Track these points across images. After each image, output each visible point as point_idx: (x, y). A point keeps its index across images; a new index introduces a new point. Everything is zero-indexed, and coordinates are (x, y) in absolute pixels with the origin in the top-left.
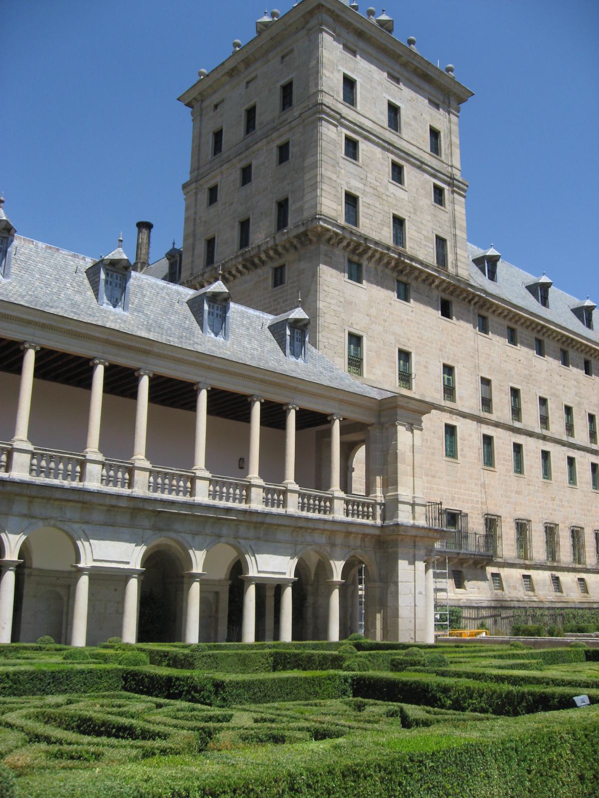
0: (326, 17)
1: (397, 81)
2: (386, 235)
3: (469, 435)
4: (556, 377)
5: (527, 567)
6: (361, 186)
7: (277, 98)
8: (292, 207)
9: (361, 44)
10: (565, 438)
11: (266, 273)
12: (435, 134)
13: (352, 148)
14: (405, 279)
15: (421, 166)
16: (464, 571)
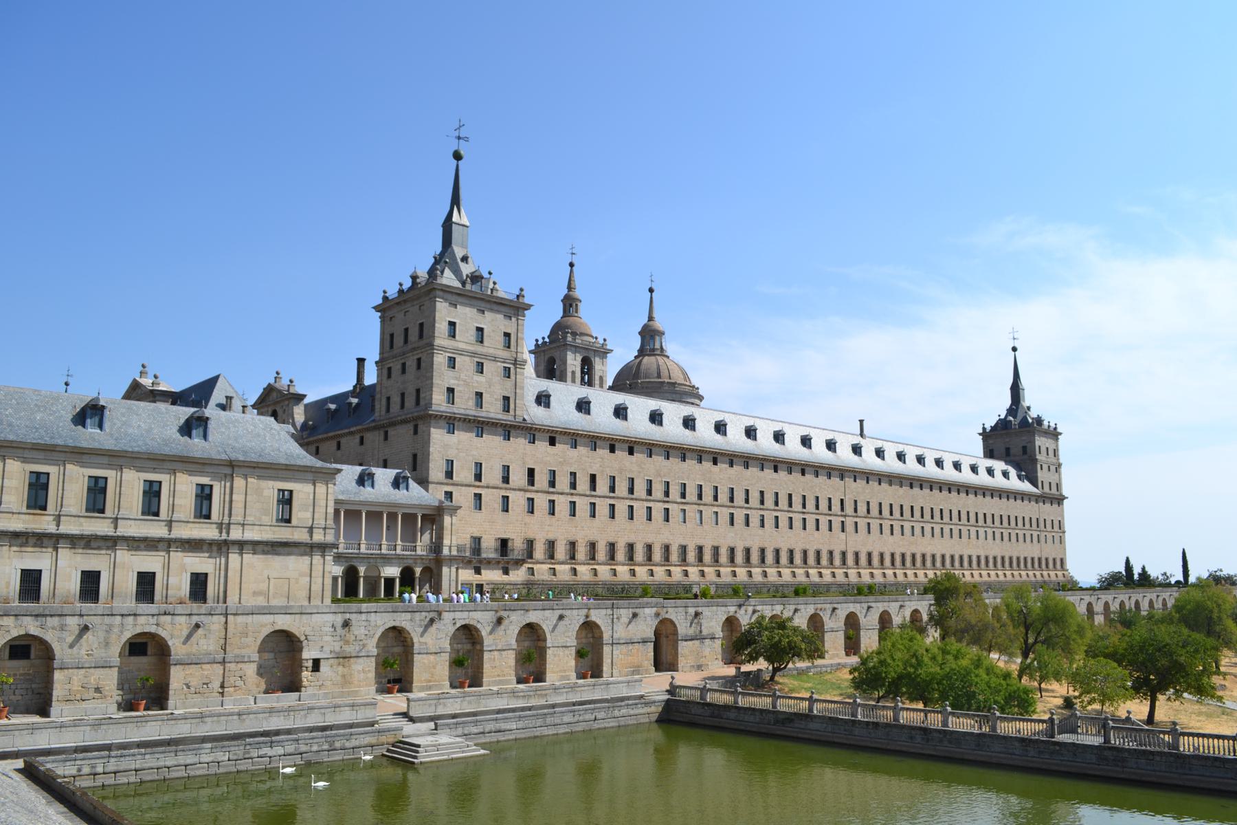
0: (438, 293)
1: (483, 312)
7: (417, 329)
8: (422, 395)
9: (460, 299)
10: (588, 493)
11: (410, 427)
12: (507, 335)
13: (452, 363)
14: (480, 426)
15: (495, 359)
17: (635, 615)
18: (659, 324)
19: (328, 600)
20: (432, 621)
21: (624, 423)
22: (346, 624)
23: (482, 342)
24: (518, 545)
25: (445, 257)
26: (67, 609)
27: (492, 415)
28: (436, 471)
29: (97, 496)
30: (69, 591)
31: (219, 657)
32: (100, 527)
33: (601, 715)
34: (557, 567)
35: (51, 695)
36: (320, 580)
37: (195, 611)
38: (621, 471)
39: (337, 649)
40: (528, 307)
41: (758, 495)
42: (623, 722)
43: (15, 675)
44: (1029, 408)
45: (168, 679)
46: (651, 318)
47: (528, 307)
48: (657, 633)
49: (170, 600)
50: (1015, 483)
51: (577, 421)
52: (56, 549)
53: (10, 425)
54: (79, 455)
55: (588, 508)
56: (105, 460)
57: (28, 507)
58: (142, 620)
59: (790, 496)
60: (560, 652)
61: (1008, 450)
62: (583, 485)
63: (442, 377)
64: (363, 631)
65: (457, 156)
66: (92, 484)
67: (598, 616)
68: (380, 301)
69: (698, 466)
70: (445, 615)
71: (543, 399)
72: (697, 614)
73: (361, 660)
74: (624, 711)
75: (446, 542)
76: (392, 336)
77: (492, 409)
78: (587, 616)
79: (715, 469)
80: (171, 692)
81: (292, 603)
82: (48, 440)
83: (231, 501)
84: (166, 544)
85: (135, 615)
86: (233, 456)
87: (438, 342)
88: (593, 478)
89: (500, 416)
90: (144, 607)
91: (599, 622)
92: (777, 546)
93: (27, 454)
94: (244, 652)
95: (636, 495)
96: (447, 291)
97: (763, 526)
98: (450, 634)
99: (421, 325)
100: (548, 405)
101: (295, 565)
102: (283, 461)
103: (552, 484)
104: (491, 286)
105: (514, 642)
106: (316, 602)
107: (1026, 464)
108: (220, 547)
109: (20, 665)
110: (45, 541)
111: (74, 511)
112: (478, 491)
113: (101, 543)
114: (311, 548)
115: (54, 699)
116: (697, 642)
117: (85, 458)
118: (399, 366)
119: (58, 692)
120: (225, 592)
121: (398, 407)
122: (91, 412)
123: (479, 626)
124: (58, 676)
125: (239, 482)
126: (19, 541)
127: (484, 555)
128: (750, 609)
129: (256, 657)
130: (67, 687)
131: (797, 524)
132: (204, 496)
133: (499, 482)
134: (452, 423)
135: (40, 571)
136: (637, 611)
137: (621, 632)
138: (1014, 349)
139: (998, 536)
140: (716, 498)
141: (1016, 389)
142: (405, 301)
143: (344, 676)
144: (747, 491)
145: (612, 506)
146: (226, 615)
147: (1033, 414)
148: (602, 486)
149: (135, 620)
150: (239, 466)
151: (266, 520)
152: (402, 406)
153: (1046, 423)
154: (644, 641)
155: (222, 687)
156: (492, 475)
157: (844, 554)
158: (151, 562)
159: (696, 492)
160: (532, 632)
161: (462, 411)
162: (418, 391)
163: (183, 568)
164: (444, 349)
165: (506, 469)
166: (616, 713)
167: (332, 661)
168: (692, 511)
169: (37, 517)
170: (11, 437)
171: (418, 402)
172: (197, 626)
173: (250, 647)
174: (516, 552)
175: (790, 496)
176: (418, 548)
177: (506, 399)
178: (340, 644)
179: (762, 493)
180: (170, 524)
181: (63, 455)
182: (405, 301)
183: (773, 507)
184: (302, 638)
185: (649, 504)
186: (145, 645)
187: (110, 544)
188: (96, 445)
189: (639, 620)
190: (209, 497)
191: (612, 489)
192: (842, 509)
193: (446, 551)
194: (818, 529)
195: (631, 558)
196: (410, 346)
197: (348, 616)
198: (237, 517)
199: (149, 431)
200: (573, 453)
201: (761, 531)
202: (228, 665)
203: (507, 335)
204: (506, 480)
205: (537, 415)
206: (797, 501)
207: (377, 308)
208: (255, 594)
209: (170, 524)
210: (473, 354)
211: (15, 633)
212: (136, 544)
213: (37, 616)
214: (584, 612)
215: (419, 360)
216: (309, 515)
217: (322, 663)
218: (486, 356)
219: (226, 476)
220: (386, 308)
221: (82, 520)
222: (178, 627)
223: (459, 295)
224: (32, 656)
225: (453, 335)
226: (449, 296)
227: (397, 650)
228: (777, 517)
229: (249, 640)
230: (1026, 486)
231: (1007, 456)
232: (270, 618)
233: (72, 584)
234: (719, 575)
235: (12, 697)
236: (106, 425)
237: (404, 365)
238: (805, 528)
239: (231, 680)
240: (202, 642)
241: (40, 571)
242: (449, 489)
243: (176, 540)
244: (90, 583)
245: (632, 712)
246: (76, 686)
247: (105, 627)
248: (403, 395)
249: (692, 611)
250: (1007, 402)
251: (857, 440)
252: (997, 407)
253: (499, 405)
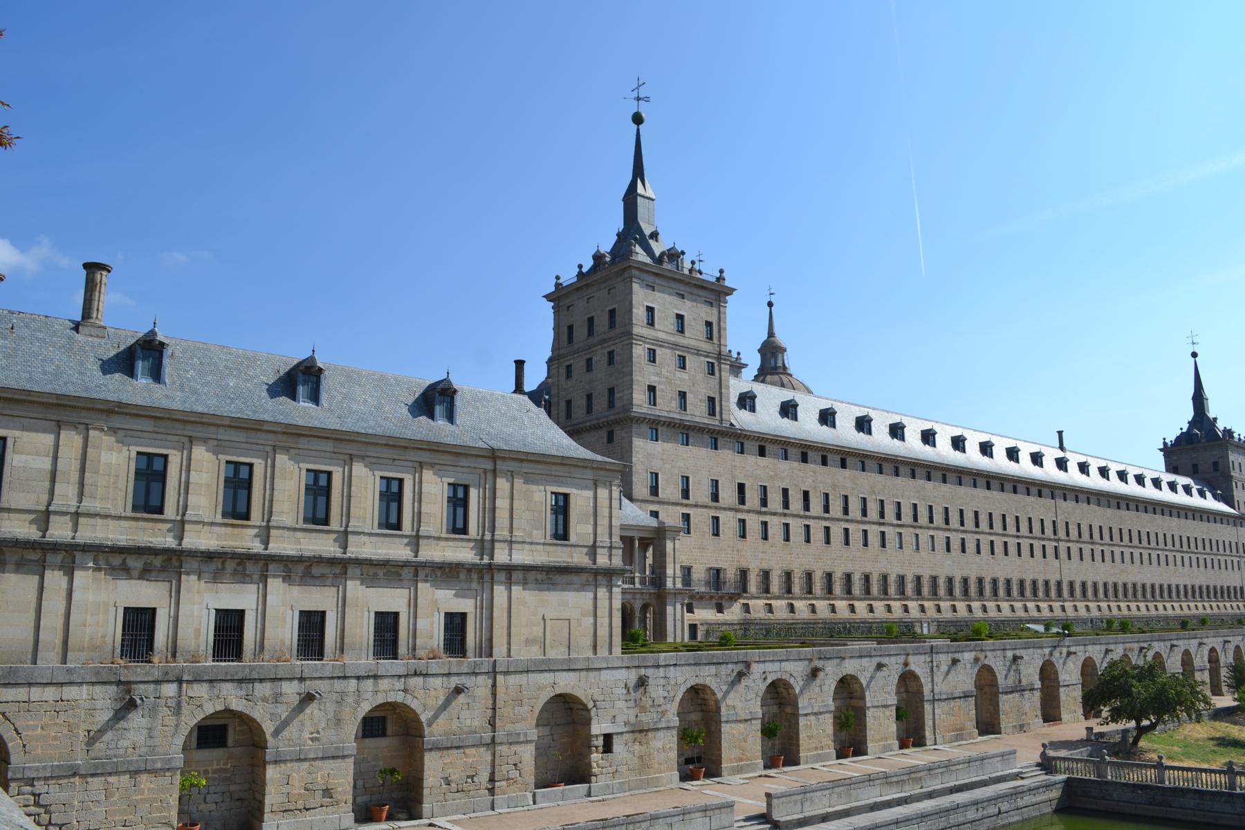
0: (635, 272)
1: (683, 297)
2: (675, 404)
3: (729, 521)
4: (796, 472)
5: (768, 599)
6: (657, 379)
7: (606, 317)
8: (617, 396)
9: (658, 281)
10: (802, 513)
11: (603, 434)
12: (709, 324)
13: (652, 357)
14: (686, 432)
15: (698, 352)
16: (724, 603)
17: (955, 662)
18: (781, 338)
19: (617, 650)
20: (741, 675)
21: (832, 430)
22: (642, 682)
23: (681, 330)
24: (731, 575)
25: (631, 232)
26: (283, 669)
27: (697, 419)
28: (641, 488)
29: (318, 502)
30: (283, 643)
31: (487, 736)
32: (322, 545)
33: (1004, 806)
34: (773, 602)
35: (262, 803)
36: (607, 620)
37: (454, 670)
38: (834, 487)
39: (632, 719)
40: (730, 291)
41: (972, 515)
42: (1027, 813)
43: (206, 772)
44: (1215, 419)
45: (422, 771)
46: (771, 334)
47: (730, 291)
48: (979, 686)
49: (420, 653)
50: (1210, 503)
51: (785, 427)
52: (264, 579)
53: (195, 392)
54: (293, 437)
55: (803, 530)
56: (328, 446)
57: (224, 515)
58: (384, 684)
59: (1004, 516)
60: (879, 713)
61: (1195, 467)
62: (796, 504)
63: (643, 374)
64: (661, 693)
65: (638, 119)
66: (311, 482)
67: (918, 665)
68: (553, 289)
69: (911, 481)
70: (756, 669)
71: (747, 401)
72: (1015, 658)
73: (660, 734)
74: (1028, 799)
75: (669, 572)
76: (570, 328)
77: (697, 412)
78: (906, 664)
79: (929, 485)
80: (426, 792)
81: (573, 656)
82: (249, 414)
83: (494, 509)
84: (412, 570)
85: (376, 677)
86: (496, 444)
87: (636, 330)
88: (806, 494)
89: (706, 421)
90: (387, 665)
91: (918, 671)
92: (994, 576)
93: (223, 434)
94: (520, 727)
95: (851, 515)
96: (642, 268)
97: (979, 552)
98: (761, 694)
99: (612, 313)
100: (753, 409)
101: (573, 604)
102: (554, 452)
103: (764, 502)
104: (690, 266)
105: (830, 701)
106: (603, 652)
107: (1216, 480)
108: (483, 575)
109: (213, 756)
110: (251, 567)
111: (288, 520)
112: (686, 511)
113: (325, 570)
114: (600, 576)
115: (267, 809)
116: (1016, 695)
117: (303, 443)
118: (583, 363)
119: (272, 798)
120: (491, 640)
121: (584, 410)
122: (302, 379)
123: (792, 681)
124: (271, 773)
125: (502, 484)
126: (214, 566)
127: (697, 589)
128: (1065, 650)
129: (533, 734)
130: (285, 790)
131: (1012, 550)
132: (458, 501)
133: (707, 499)
134: (657, 427)
135: (241, 613)
136: (957, 656)
137: (942, 688)
138: (1194, 355)
139: (1202, 562)
140: (931, 521)
141: (1199, 399)
142: (587, 286)
143: (641, 757)
144: (961, 511)
145: (827, 529)
146: (494, 673)
147: (1221, 425)
148: (816, 507)
149: (376, 685)
150: (504, 459)
151: (538, 535)
152: (589, 409)
153: (1236, 435)
154: (966, 696)
155: (492, 780)
156: (700, 492)
157: (1059, 584)
158: (393, 599)
159: (911, 513)
160: (848, 689)
161: (666, 414)
162: (611, 391)
163: (435, 605)
164: (643, 338)
165: (715, 483)
166: (1020, 803)
167: (626, 737)
168: (908, 534)
169: (236, 530)
170: (200, 409)
171: (611, 404)
172: (458, 690)
173: (523, 720)
174: (728, 585)
175: (1004, 516)
176: (637, 580)
177: (711, 400)
178: (632, 712)
179: (976, 513)
180: (416, 541)
181: (271, 436)
182: (587, 286)
183: (987, 530)
184: (590, 705)
185: (865, 527)
186: (383, 720)
187: (337, 570)
188: (316, 424)
189: (960, 665)
190: (465, 502)
191: (827, 509)
192: (1055, 533)
193: (669, 584)
194: (1032, 556)
195: (849, 592)
196: (597, 338)
197: (643, 672)
198: (502, 532)
199: (379, 407)
200: (784, 466)
201: (977, 558)
202: (498, 748)
203: (709, 324)
204: (715, 497)
205: (741, 419)
206: (1010, 522)
207: (548, 297)
208: (528, 642)
209: (416, 541)
210: (675, 346)
211: (210, 709)
212: (372, 571)
213: (240, 681)
214: (901, 659)
215: (611, 355)
216: (590, 529)
217: (616, 740)
218: (687, 348)
219: (485, 471)
220: (560, 297)
221: (299, 535)
222: (433, 693)
223: (656, 275)
224: (230, 742)
225: (651, 323)
226: (644, 276)
227: (695, 717)
228: (992, 542)
229: (526, 708)
230: (1222, 507)
231: (1193, 472)
232: (547, 678)
233: (284, 631)
234: (939, 610)
235: (202, 807)
236: (324, 397)
237: (589, 361)
238: (1020, 555)
239: (503, 769)
240: (465, 714)
241: (241, 613)
242: (654, 508)
243: (424, 565)
244: (312, 627)
245: (1034, 800)
246: (297, 788)
247: (335, 697)
248: (589, 397)
249: (1010, 654)
250: (1190, 414)
251: (1060, 454)
252: (1179, 419)
253: (704, 407)
